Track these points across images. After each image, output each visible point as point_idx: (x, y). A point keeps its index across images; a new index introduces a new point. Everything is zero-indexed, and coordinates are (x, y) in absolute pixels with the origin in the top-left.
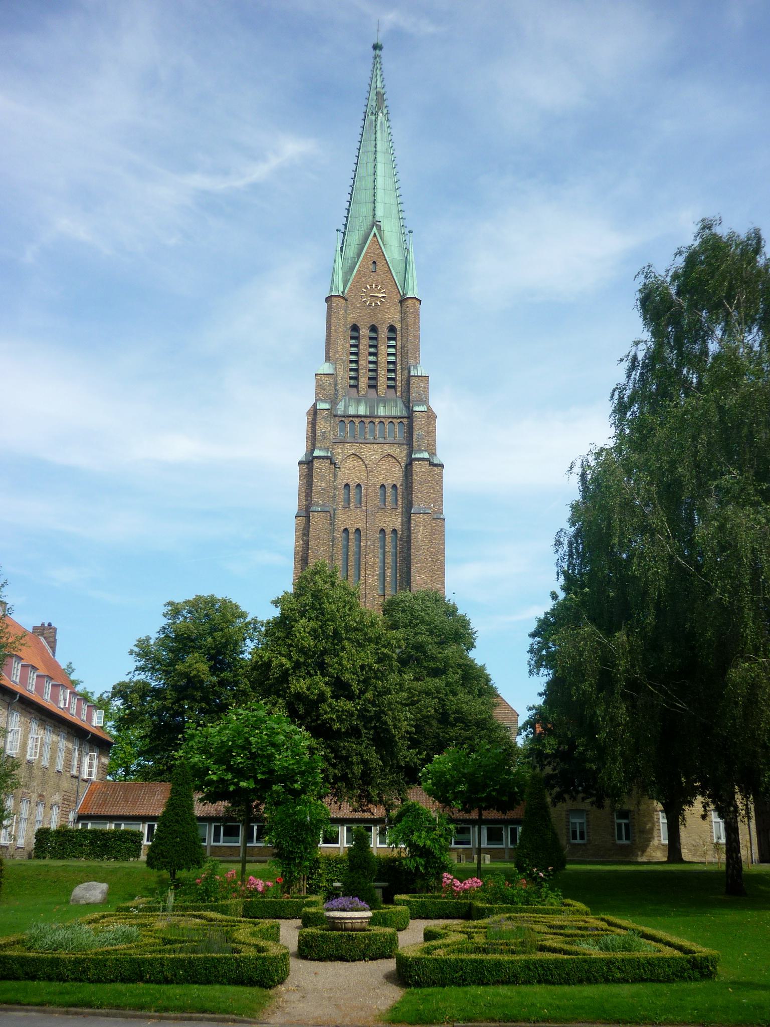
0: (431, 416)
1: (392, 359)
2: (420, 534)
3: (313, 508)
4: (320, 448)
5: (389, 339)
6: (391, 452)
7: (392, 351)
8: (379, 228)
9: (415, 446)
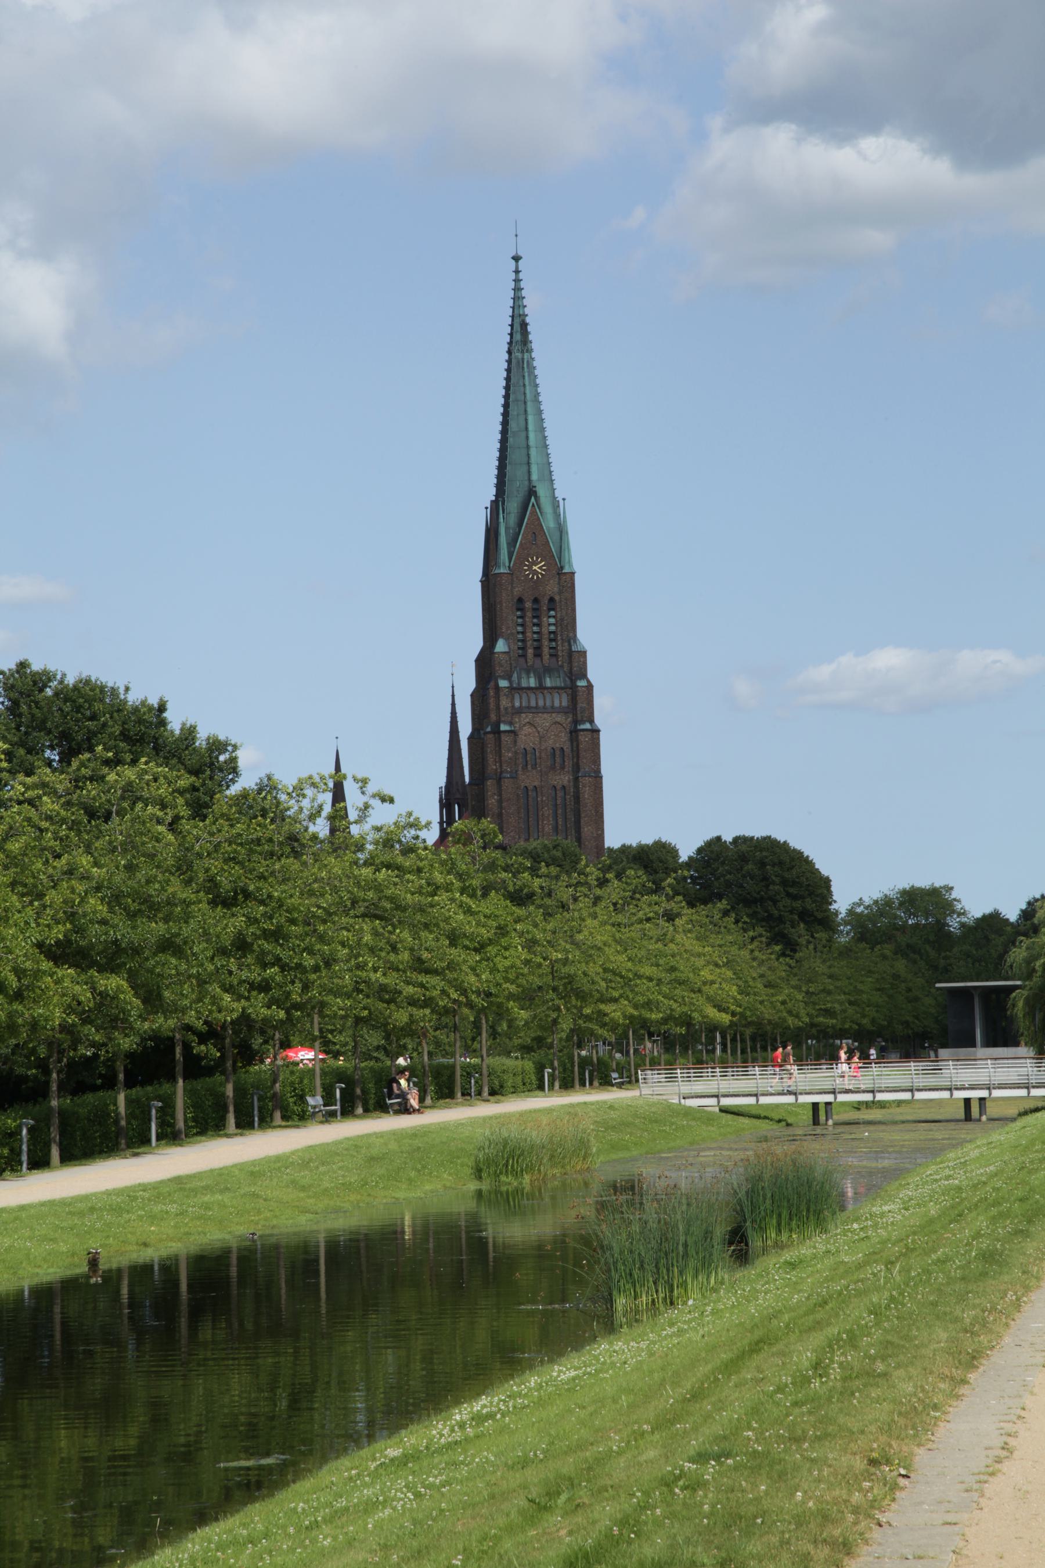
0: (590, 687)
1: (553, 628)
2: (586, 793)
3: (504, 775)
4: (505, 723)
5: (550, 610)
6: (559, 719)
7: (552, 620)
8: (535, 492)
9: (579, 718)
